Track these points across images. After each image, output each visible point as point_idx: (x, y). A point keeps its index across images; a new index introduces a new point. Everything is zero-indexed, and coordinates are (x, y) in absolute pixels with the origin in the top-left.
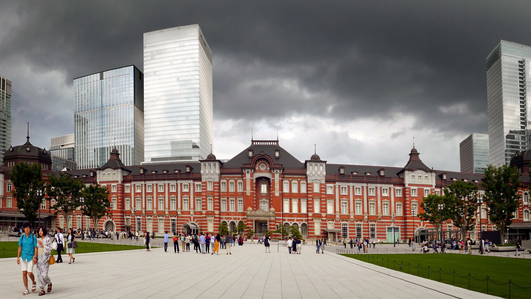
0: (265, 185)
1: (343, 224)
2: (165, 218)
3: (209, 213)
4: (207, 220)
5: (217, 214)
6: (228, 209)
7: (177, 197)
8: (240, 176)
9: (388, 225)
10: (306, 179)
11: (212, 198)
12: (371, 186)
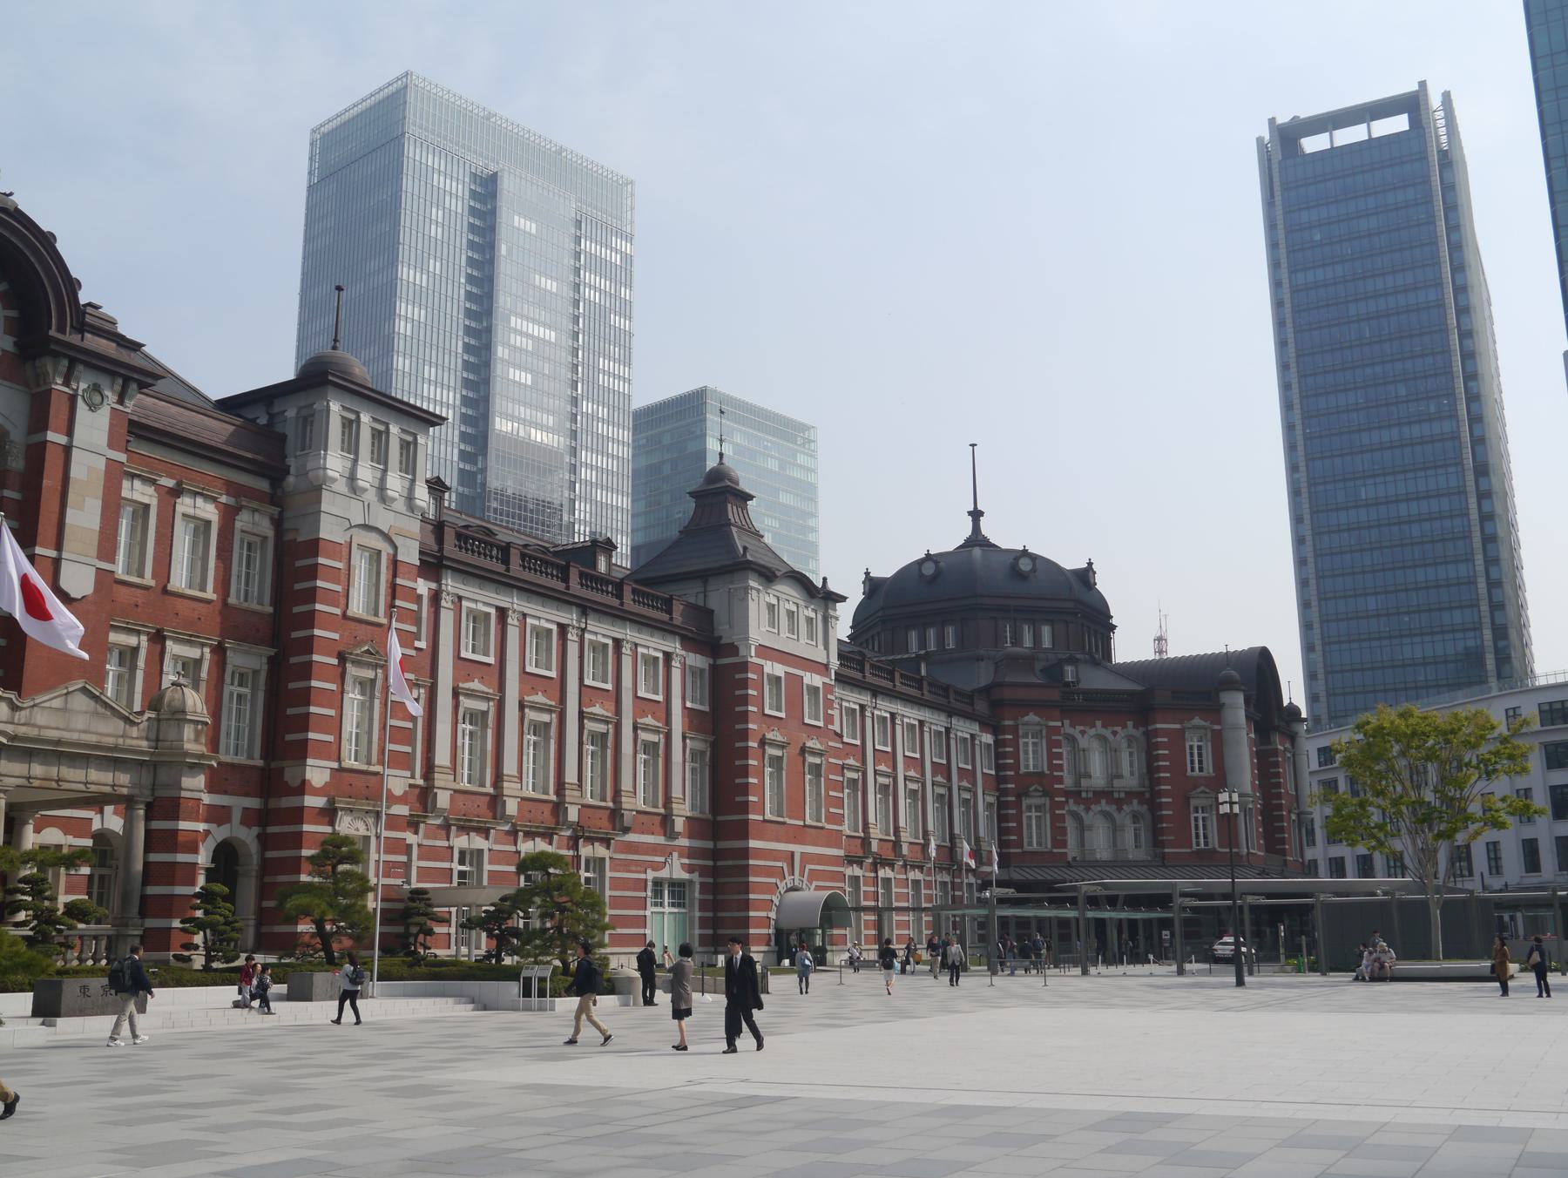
1: (462, 853)
10: (275, 511)
12: (601, 631)
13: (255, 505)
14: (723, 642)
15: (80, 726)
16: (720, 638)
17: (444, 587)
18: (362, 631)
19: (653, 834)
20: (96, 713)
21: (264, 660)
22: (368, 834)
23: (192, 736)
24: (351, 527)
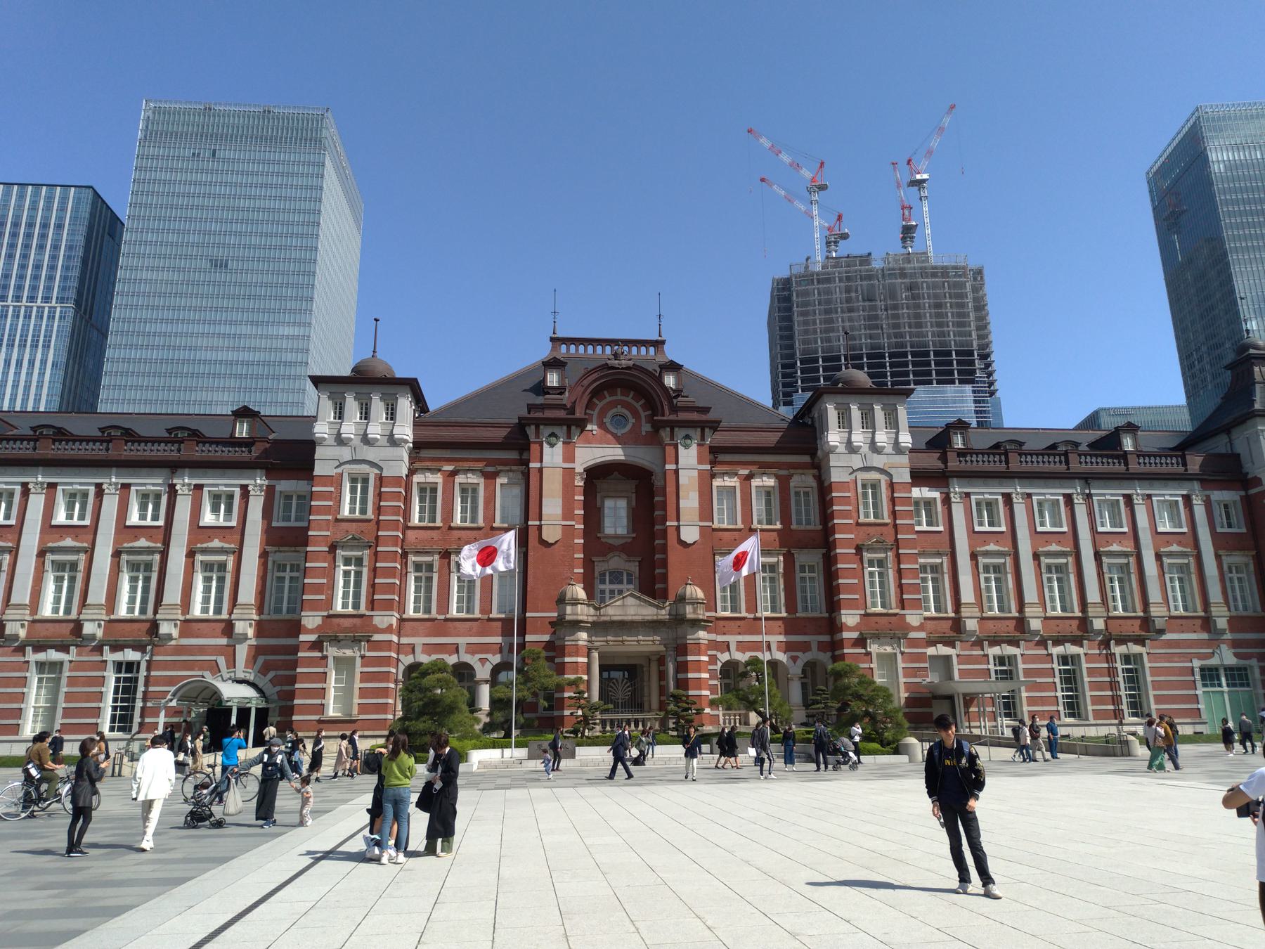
0: (622, 504)
2: (79, 654)
3: (339, 625)
4: (325, 658)
5: (384, 626)
6: (444, 605)
7: (164, 554)
8: (513, 455)
9: (1201, 657)
10: (815, 471)
11: (366, 554)
13: (800, 471)
14: (1250, 476)
15: (633, 613)
16: (1248, 473)
17: (952, 490)
18: (872, 530)
19: (1195, 632)
20: (640, 605)
21: (821, 556)
22: (895, 651)
23: (691, 611)
24: (854, 471)
